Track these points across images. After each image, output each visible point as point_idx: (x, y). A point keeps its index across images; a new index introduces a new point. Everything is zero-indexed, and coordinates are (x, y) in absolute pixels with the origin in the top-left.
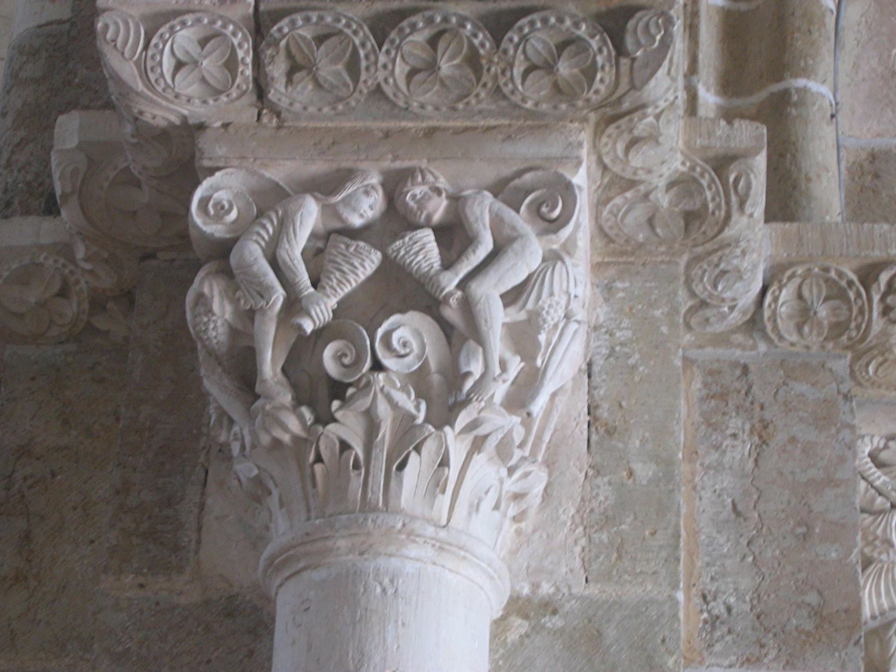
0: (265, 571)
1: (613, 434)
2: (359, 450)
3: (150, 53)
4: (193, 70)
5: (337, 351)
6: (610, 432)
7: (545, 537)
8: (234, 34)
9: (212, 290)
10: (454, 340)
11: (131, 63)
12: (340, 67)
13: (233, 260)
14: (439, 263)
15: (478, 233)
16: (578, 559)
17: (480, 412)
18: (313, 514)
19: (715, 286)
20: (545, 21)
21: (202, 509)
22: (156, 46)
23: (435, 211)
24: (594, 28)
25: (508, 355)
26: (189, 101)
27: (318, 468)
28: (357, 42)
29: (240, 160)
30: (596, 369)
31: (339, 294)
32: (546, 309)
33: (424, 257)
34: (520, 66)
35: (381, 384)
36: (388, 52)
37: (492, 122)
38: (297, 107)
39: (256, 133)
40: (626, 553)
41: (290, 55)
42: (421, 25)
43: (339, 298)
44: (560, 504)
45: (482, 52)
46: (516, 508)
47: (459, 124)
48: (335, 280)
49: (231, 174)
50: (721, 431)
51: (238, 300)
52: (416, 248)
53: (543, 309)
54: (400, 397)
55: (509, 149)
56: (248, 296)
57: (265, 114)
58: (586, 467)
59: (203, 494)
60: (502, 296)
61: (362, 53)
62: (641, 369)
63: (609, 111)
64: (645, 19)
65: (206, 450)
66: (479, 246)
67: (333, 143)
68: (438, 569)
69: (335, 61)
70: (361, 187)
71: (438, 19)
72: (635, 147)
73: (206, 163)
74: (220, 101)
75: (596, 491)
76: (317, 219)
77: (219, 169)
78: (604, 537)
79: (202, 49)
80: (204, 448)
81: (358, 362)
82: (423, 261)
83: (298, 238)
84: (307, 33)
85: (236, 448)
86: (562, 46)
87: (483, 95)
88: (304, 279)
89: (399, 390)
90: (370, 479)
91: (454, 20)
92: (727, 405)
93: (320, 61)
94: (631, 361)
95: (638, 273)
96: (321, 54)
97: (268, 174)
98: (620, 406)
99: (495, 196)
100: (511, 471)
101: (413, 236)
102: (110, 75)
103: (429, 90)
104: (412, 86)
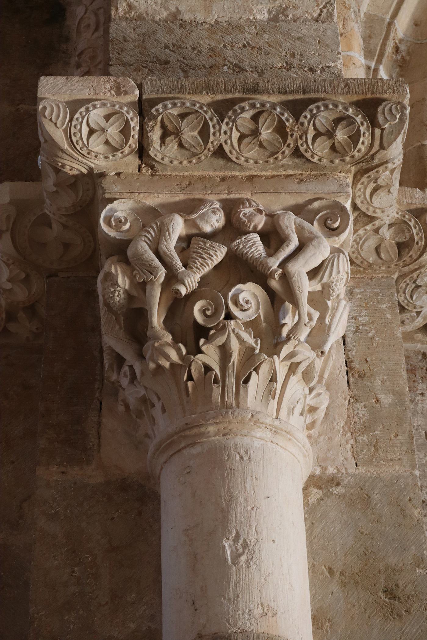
0: (154, 454)
1: (364, 377)
2: (217, 371)
3: (73, 124)
4: (101, 135)
5: (202, 307)
6: (362, 376)
7: (327, 439)
8: (128, 112)
9: (116, 271)
11: (61, 130)
12: (196, 133)
13: (130, 253)
15: (289, 235)
16: (349, 452)
17: (295, 348)
19: (411, 297)
20: (326, 106)
21: (100, 426)
22: (77, 119)
23: (260, 223)
24: (357, 110)
25: (312, 311)
26: (96, 157)
27: (190, 384)
28: (207, 118)
30: (348, 340)
32: (335, 283)
33: (256, 249)
35: (233, 327)
36: (227, 124)
37: (291, 172)
38: (167, 160)
40: (380, 447)
41: (163, 126)
42: (247, 108)
43: (201, 274)
44: (334, 419)
45: (287, 124)
46: (311, 418)
47: (269, 173)
48: (198, 263)
50: (414, 391)
51: (135, 276)
52: (250, 244)
54: (245, 336)
56: (142, 274)
58: (348, 397)
59: (100, 416)
60: (308, 273)
61: (211, 124)
62: (377, 339)
63: (365, 165)
64: (389, 106)
66: (291, 243)
67: (189, 184)
68: (274, 446)
69: (193, 129)
71: (258, 105)
72: (378, 192)
73: (107, 196)
74: (116, 156)
75: (357, 411)
77: (116, 199)
78: (365, 438)
79: (107, 122)
80: (98, 388)
81: (216, 313)
82: (255, 252)
84: (175, 112)
85: (125, 382)
86: (337, 121)
87: (287, 152)
88: (178, 262)
90: (226, 389)
91: (268, 105)
92: (416, 376)
93: (184, 129)
94: (370, 335)
95: (368, 284)
96: (184, 125)
97: (148, 203)
98: (366, 360)
99: (296, 215)
100: (311, 390)
102: (46, 141)
103: (254, 149)
104: (242, 146)
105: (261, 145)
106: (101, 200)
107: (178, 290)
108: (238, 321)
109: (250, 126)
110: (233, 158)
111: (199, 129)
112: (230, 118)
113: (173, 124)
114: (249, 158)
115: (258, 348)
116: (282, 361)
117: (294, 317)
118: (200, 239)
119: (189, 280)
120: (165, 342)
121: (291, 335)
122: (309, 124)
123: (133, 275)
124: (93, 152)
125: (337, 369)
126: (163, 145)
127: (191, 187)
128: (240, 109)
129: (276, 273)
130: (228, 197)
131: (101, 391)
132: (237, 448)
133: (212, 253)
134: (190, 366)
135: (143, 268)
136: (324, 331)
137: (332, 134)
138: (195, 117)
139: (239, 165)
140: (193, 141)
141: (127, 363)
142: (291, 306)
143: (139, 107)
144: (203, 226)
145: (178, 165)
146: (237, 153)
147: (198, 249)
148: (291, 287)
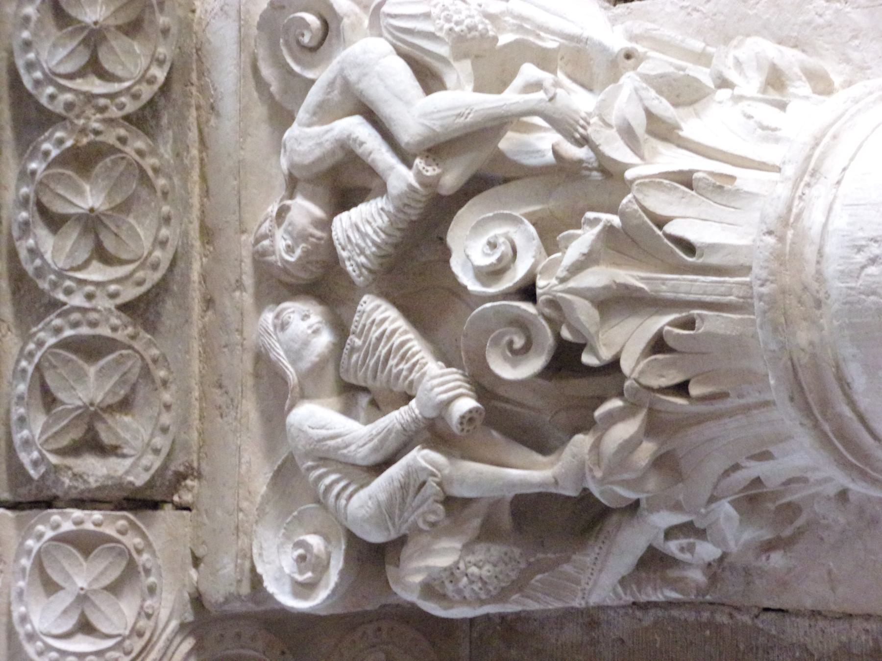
2: (661, 322)
5: (506, 359)
7: (857, 42)
10: (499, 173)
12: (92, 370)
13: (376, 537)
14: (379, 199)
15: (337, 141)
17: (609, 126)
18: (767, 397)
20: (27, 45)
21: (820, 613)
23: (309, 213)
25: (518, 81)
26: (149, 616)
27: (695, 390)
29: (241, 534)
31: (423, 358)
32: (452, 25)
33: (369, 223)
34: (93, 84)
35: (554, 281)
36: (68, 292)
37: (193, 135)
38: (159, 441)
39: (206, 511)
41: (74, 450)
44: (809, 23)
45: (69, 143)
46: (798, 83)
47: (196, 190)
49: (261, 548)
51: (433, 525)
52: (355, 237)
53: (451, 29)
55: (229, 106)
56: (425, 508)
57: (180, 497)
59: (798, 614)
61: (68, 333)
65: (735, 613)
66: (354, 136)
67: (220, 386)
69: (81, 377)
70: (277, 336)
71: (24, 215)
74: (148, 565)
76: (323, 405)
77: (253, 569)
79: (62, 588)
80: (731, 616)
81: (521, 324)
83: (342, 430)
85: (707, 551)
87: (140, 144)
89: (564, 253)
90: (708, 299)
91: (24, 190)
93: (80, 399)
97: (263, 489)
100: (724, 83)
101: (340, 244)
103: (132, 228)
104: (124, 256)
105: (125, 207)
106: (257, 603)
107: (462, 417)
108: (540, 268)
109: (75, 235)
110: (157, 276)
111: (80, 362)
112: (55, 285)
113: (67, 426)
114: (156, 239)
115: (605, 217)
116: (642, 158)
117: (538, 128)
118: (346, 362)
119: (438, 390)
120: (590, 451)
121: (577, 136)
122: (70, 90)
123: (426, 527)
124: (135, 623)
125: (688, 18)
126: (119, 451)
127: (226, 382)
128: (33, 261)
129: (425, 173)
130: (251, 290)
131: (738, 609)
132: (851, 271)
133: (375, 334)
134: (650, 389)
135: (411, 505)
136: (579, 51)
137: (92, 32)
138: (52, 371)
139: (173, 263)
140: (111, 377)
141: (660, 543)
142: (510, 134)
143: (31, 508)
144: (316, 353)
145: (173, 413)
146: (142, 266)
147: (368, 365)
148: (456, 134)
